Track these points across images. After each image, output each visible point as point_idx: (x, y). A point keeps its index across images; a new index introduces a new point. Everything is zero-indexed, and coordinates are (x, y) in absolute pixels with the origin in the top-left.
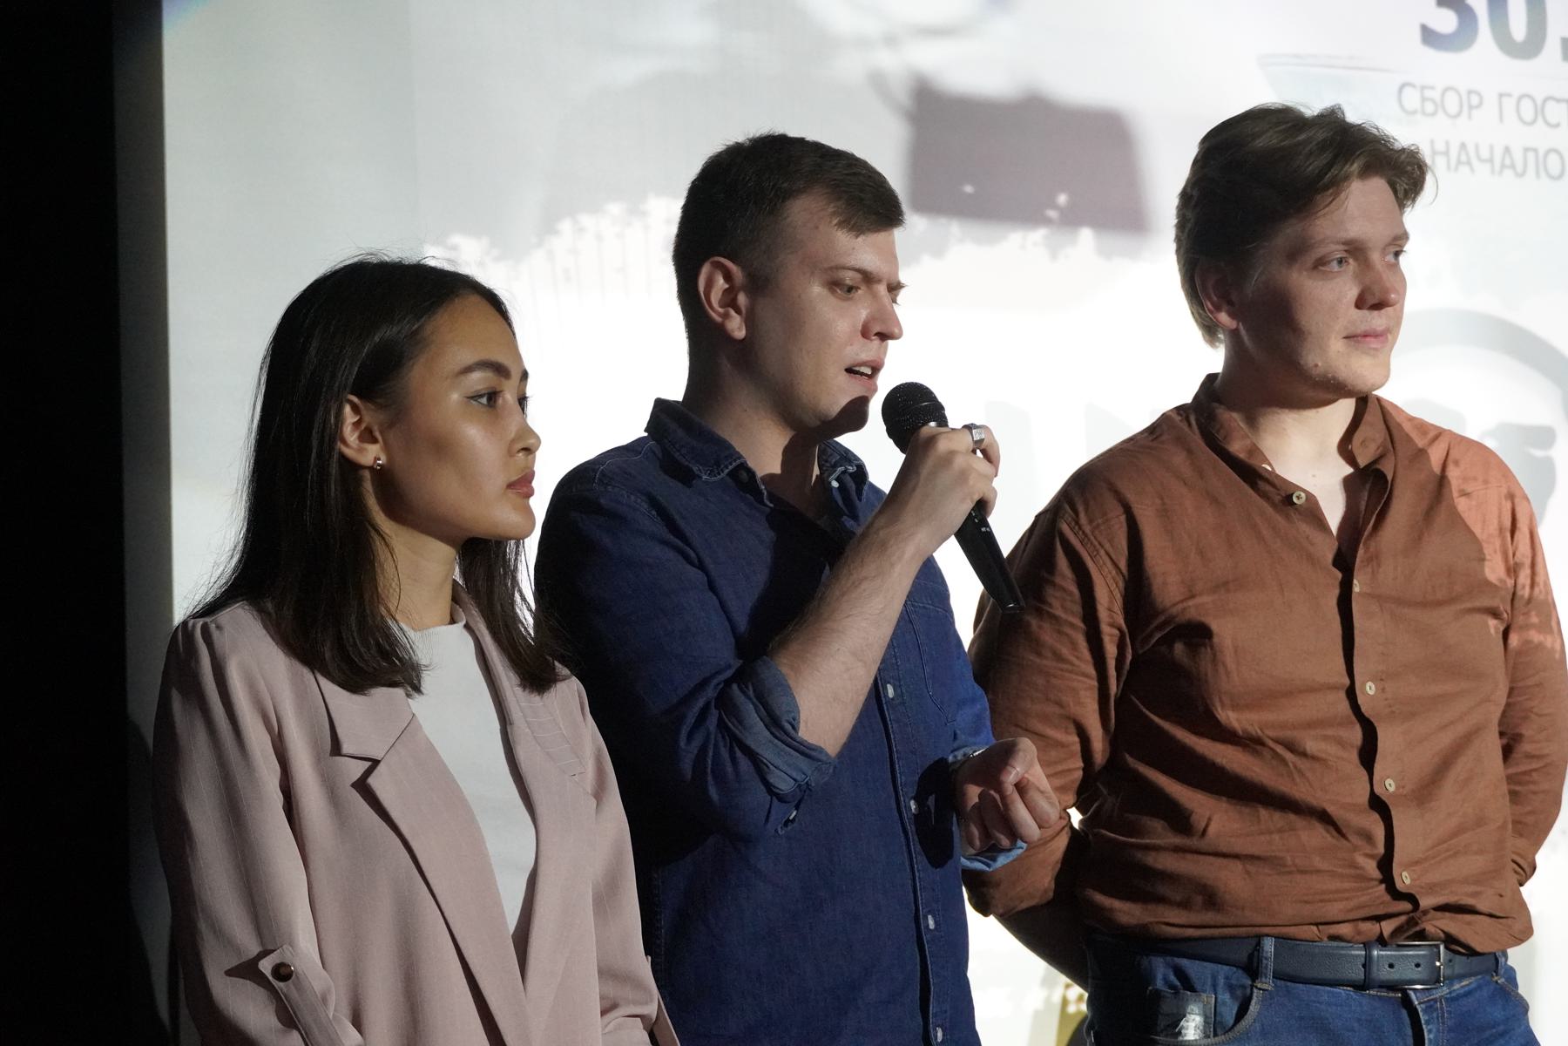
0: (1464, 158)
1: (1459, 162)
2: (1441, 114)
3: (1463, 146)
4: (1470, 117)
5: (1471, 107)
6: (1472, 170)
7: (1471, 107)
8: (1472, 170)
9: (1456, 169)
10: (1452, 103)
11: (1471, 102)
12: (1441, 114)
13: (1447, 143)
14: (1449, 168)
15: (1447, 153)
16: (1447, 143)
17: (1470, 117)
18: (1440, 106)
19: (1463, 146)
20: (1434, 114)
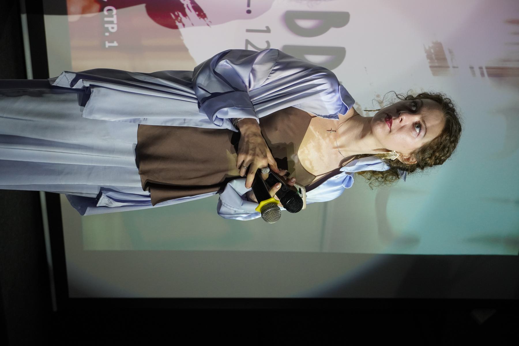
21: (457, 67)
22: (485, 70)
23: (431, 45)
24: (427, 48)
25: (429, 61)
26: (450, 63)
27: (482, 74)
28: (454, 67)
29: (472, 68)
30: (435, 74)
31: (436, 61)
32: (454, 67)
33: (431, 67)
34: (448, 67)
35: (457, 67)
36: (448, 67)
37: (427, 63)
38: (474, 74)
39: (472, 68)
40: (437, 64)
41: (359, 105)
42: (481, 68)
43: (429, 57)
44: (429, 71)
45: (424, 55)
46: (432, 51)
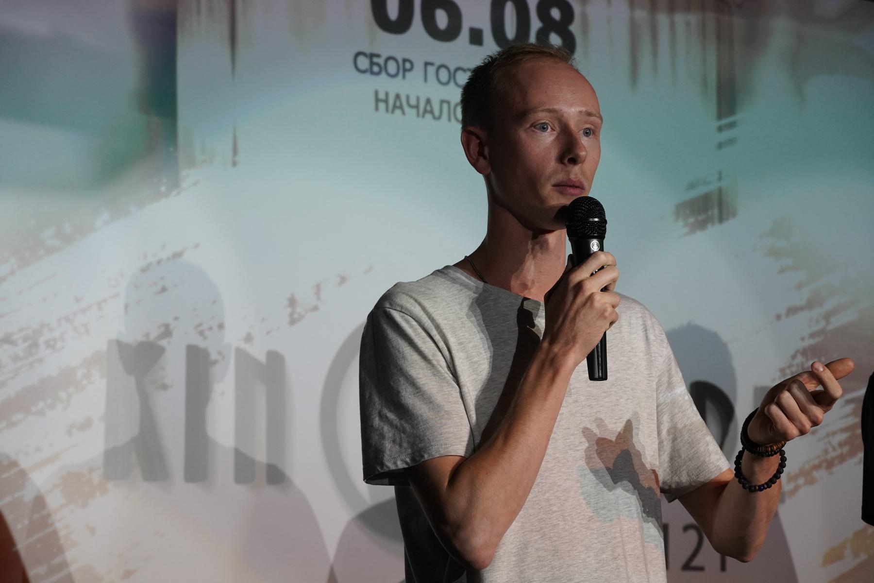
0: (398, 104)
1: (395, 107)
2: (383, 74)
3: (398, 97)
4: (404, 77)
5: (405, 70)
6: (404, 113)
7: (405, 70)
8: (404, 113)
9: (393, 112)
10: (392, 67)
11: (405, 67)
12: (383, 74)
13: (387, 94)
14: (387, 110)
15: (386, 101)
16: (387, 94)
17: (404, 77)
18: (383, 69)
19: (398, 97)
20: (379, 73)
21: (720, 173)
22: (724, 122)
23: (680, 223)
24: (686, 230)
25: (709, 226)
26: (713, 187)
27: (732, 125)
28: (720, 179)
29: (720, 146)
30: (734, 214)
31: (710, 213)
32: (720, 179)
33: (721, 220)
34: (720, 191)
35: (720, 173)
36: (720, 191)
37: (714, 230)
38: (731, 141)
39: (720, 146)
40: (716, 211)
41: (797, 352)
42: (720, 129)
43: (702, 225)
44: (730, 224)
45: (700, 235)
46: (691, 220)
